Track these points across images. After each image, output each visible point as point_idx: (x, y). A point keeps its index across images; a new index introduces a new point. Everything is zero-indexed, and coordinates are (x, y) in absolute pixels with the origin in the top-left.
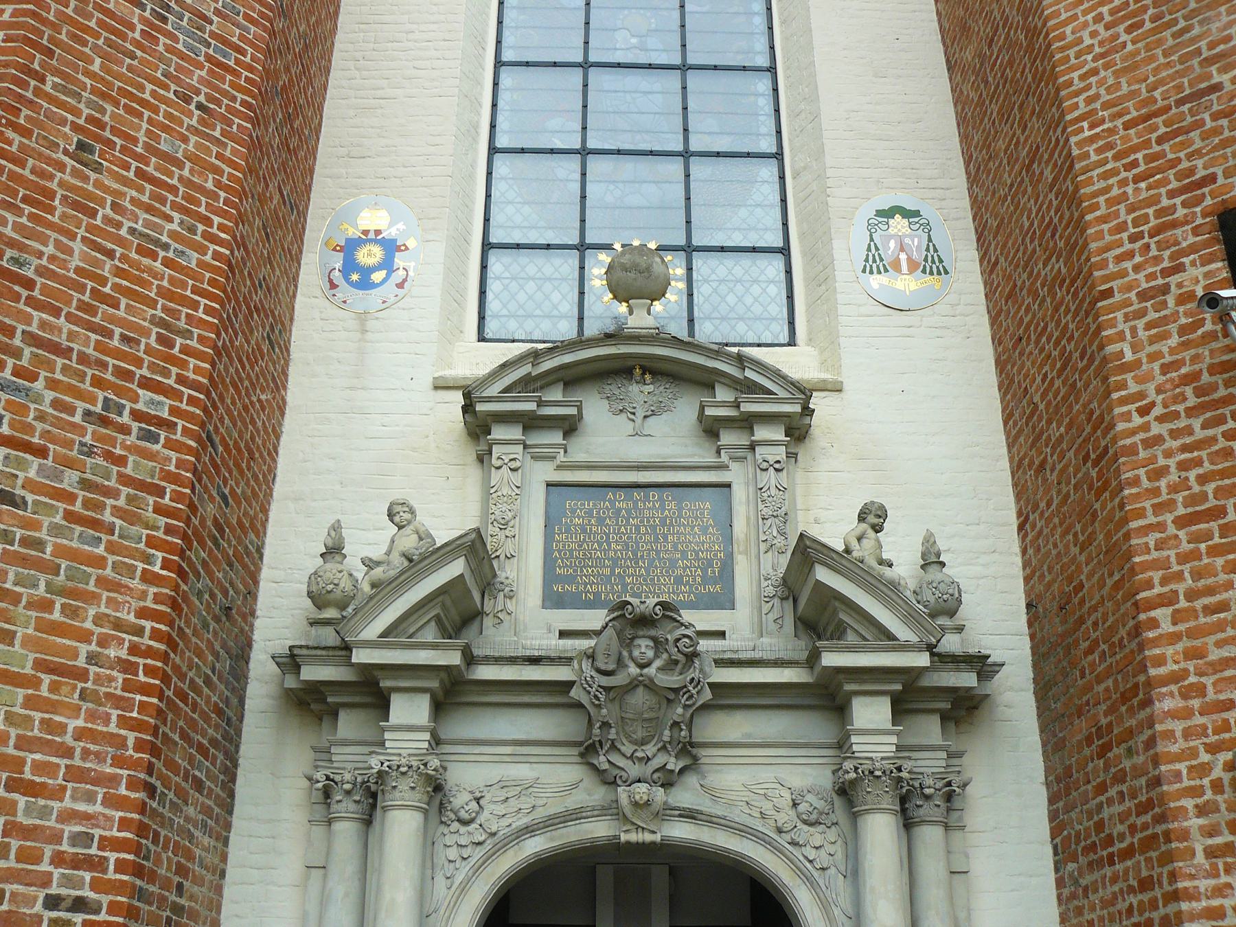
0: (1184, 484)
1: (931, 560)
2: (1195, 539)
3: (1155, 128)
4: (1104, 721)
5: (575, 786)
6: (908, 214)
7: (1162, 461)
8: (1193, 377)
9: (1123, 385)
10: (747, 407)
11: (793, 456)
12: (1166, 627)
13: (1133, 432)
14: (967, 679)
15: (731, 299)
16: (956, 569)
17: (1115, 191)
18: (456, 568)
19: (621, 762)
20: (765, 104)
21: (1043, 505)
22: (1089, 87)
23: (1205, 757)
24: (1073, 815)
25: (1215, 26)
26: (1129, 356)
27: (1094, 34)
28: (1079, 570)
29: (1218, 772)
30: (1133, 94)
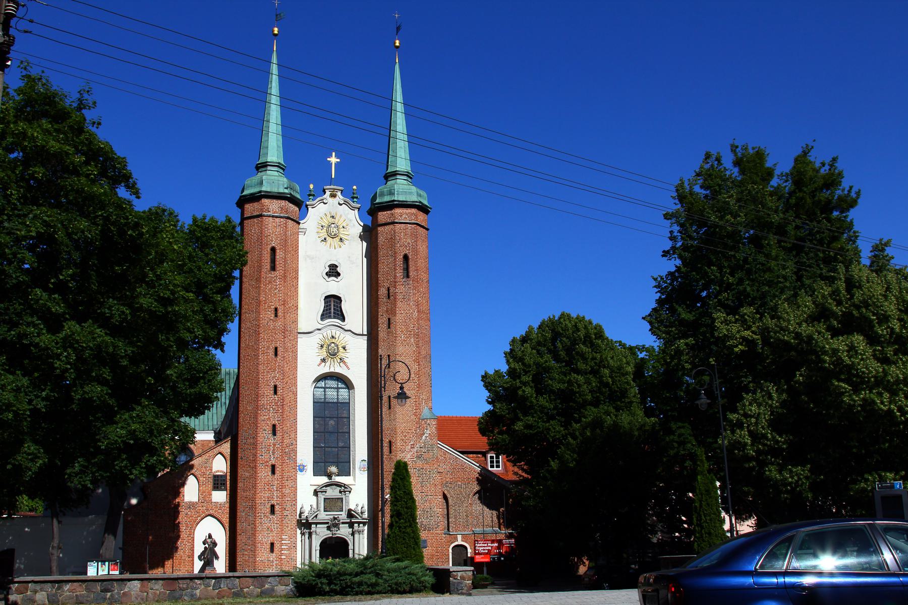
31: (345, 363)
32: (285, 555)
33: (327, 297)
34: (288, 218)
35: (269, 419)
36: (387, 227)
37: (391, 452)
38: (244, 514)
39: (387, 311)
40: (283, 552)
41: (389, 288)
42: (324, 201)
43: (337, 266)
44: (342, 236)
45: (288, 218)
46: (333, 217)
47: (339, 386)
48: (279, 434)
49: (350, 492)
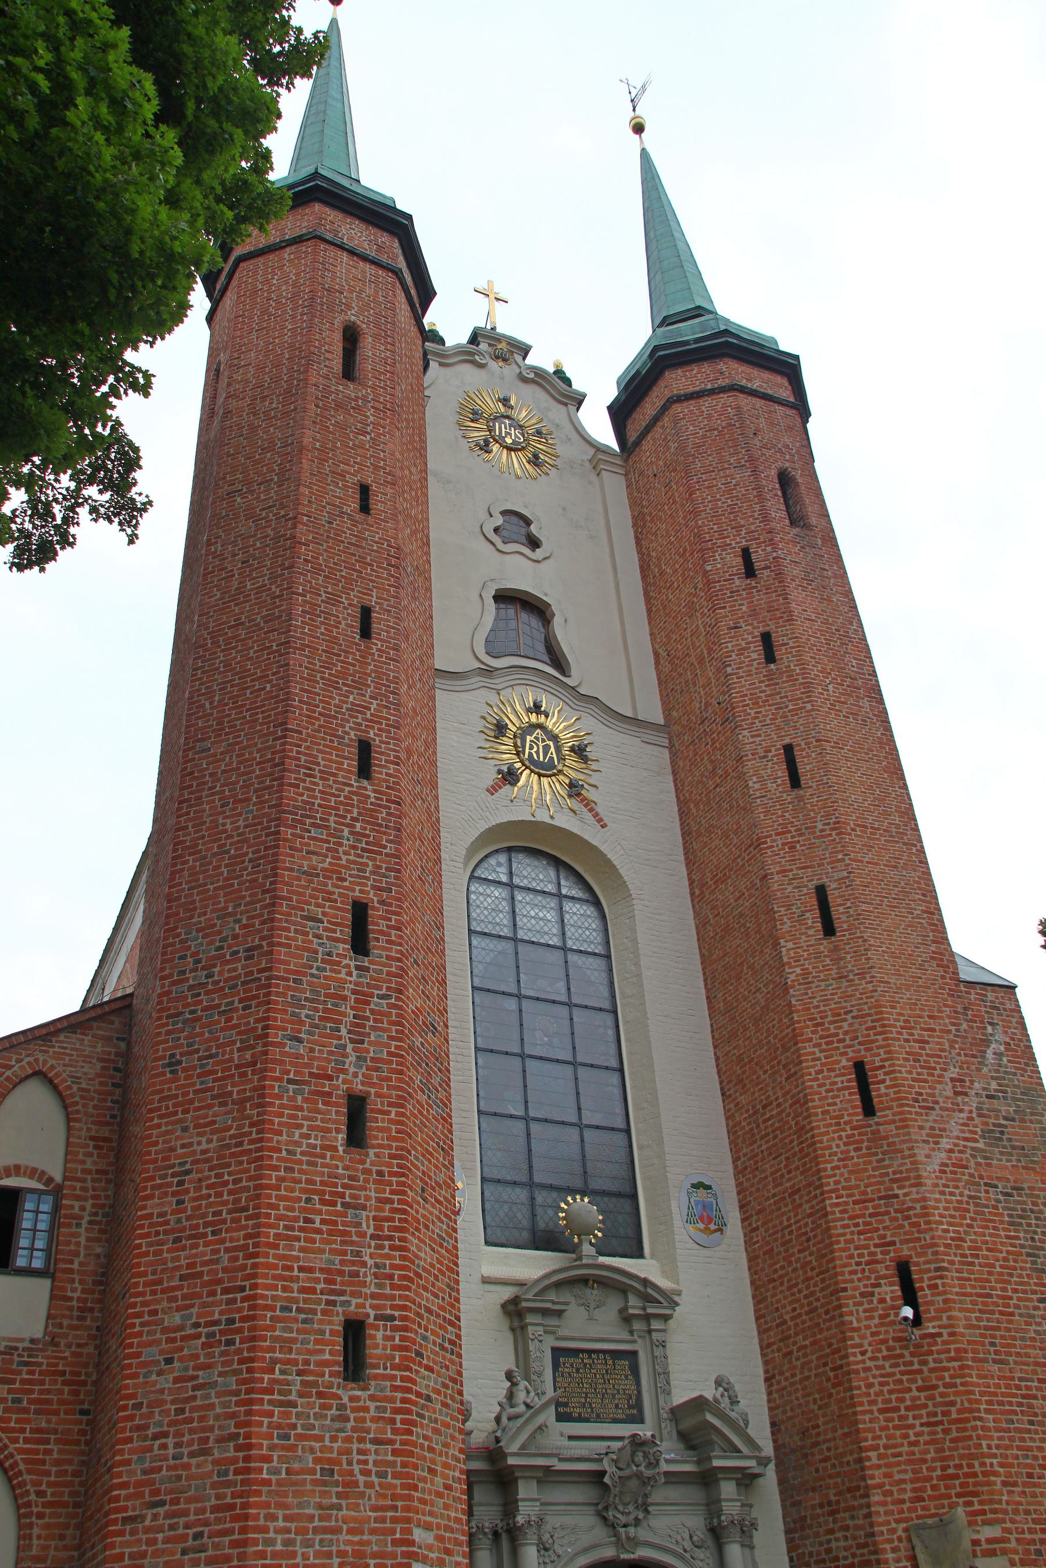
0: (880, 1393)
2: (887, 1420)
3: (867, 1208)
4: (833, 1498)
5: (593, 1527)
7: (871, 1380)
8: (884, 1341)
9: (852, 1338)
10: (650, 1311)
12: (875, 1461)
13: (857, 1363)
17: (848, 1237)
19: (619, 1516)
21: (787, 1374)
22: (835, 1175)
23: (894, 1525)
24: (807, 1542)
25: (895, 1163)
26: (855, 1324)
27: (838, 1146)
28: (816, 1417)
29: (900, 1533)
30: (857, 1187)
31: (588, 803)
36: (706, 403)
37: (869, 1109)
38: (165, 1382)
39: (754, 613)
41: (746, 554)
46: (505, 401)
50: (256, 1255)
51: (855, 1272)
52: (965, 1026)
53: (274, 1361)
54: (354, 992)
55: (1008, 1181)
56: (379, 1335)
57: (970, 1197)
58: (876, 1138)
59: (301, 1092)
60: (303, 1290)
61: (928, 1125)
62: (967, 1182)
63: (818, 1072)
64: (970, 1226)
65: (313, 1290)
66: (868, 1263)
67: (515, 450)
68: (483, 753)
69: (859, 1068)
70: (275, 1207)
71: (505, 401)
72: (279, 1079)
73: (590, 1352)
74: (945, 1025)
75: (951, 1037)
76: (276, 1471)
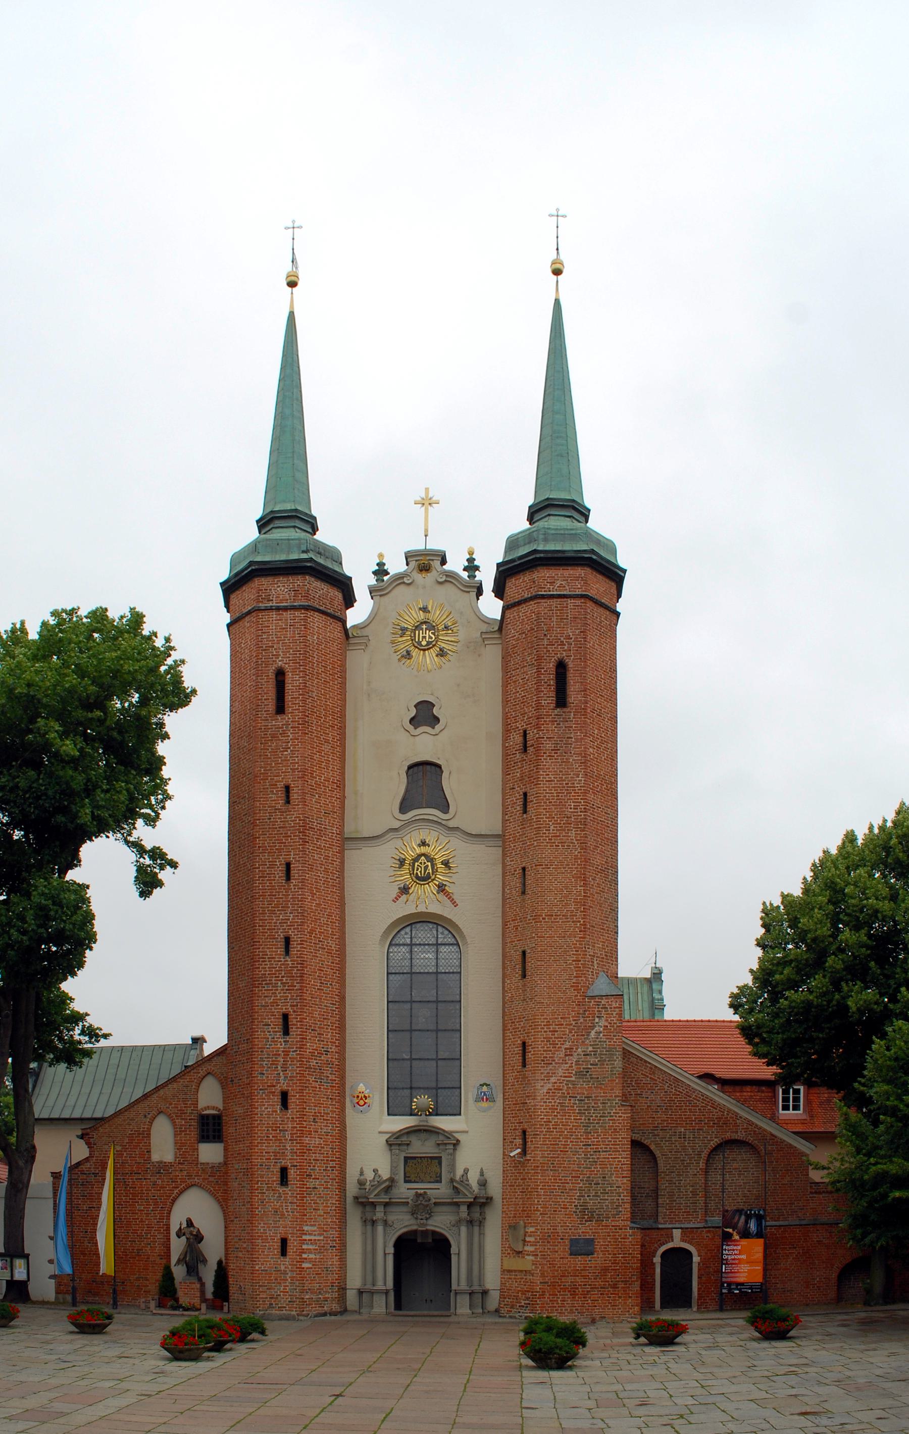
1: (482, 1174)
6: (487, 1085)
11: (455, 1149)
14: (484, 1200)
15: (447, 1101)
16: (488, 1175)
18: (387, 1183)
20: (458, 1040)
31: (448, 895)
32: (310, 1261)
33: (410, 767)
34: (307, 608)
35: (275, 1003)
37: (524, 1065)
40: (304, 1256)
42: (405, 580)
43: (433, 705)
44: (443, 645)
45: (307, 608)
46: (425, 609)
47: (440, 941)
48: (293, 1030)
49: (454, 1145)
50: (251, 1149)
51: (508, 1133)
52: (582, 1020)
53: (258, 1181)
54: (283, 1052)
55: (584, 1094)
56: (292, 1171)
57: (559, 1103)
58: (524, 1077)
59: (265, 1093)
60: (267, 1159)
61: (546, 1072)
62: (559, 1097)
63: (510, 1045)
64: (557, 1116)
65: (270, 1159)
66: (514, 1130)
67: (428, 649)
68: (393, 879)
69: (524, 1044)
70: (257, 1133)
71: (425, 609)
72: (257, 1089)
73: (421, 1157)
74: (570, 1021)
75: (572, 1027)
76: (260, 1212)
